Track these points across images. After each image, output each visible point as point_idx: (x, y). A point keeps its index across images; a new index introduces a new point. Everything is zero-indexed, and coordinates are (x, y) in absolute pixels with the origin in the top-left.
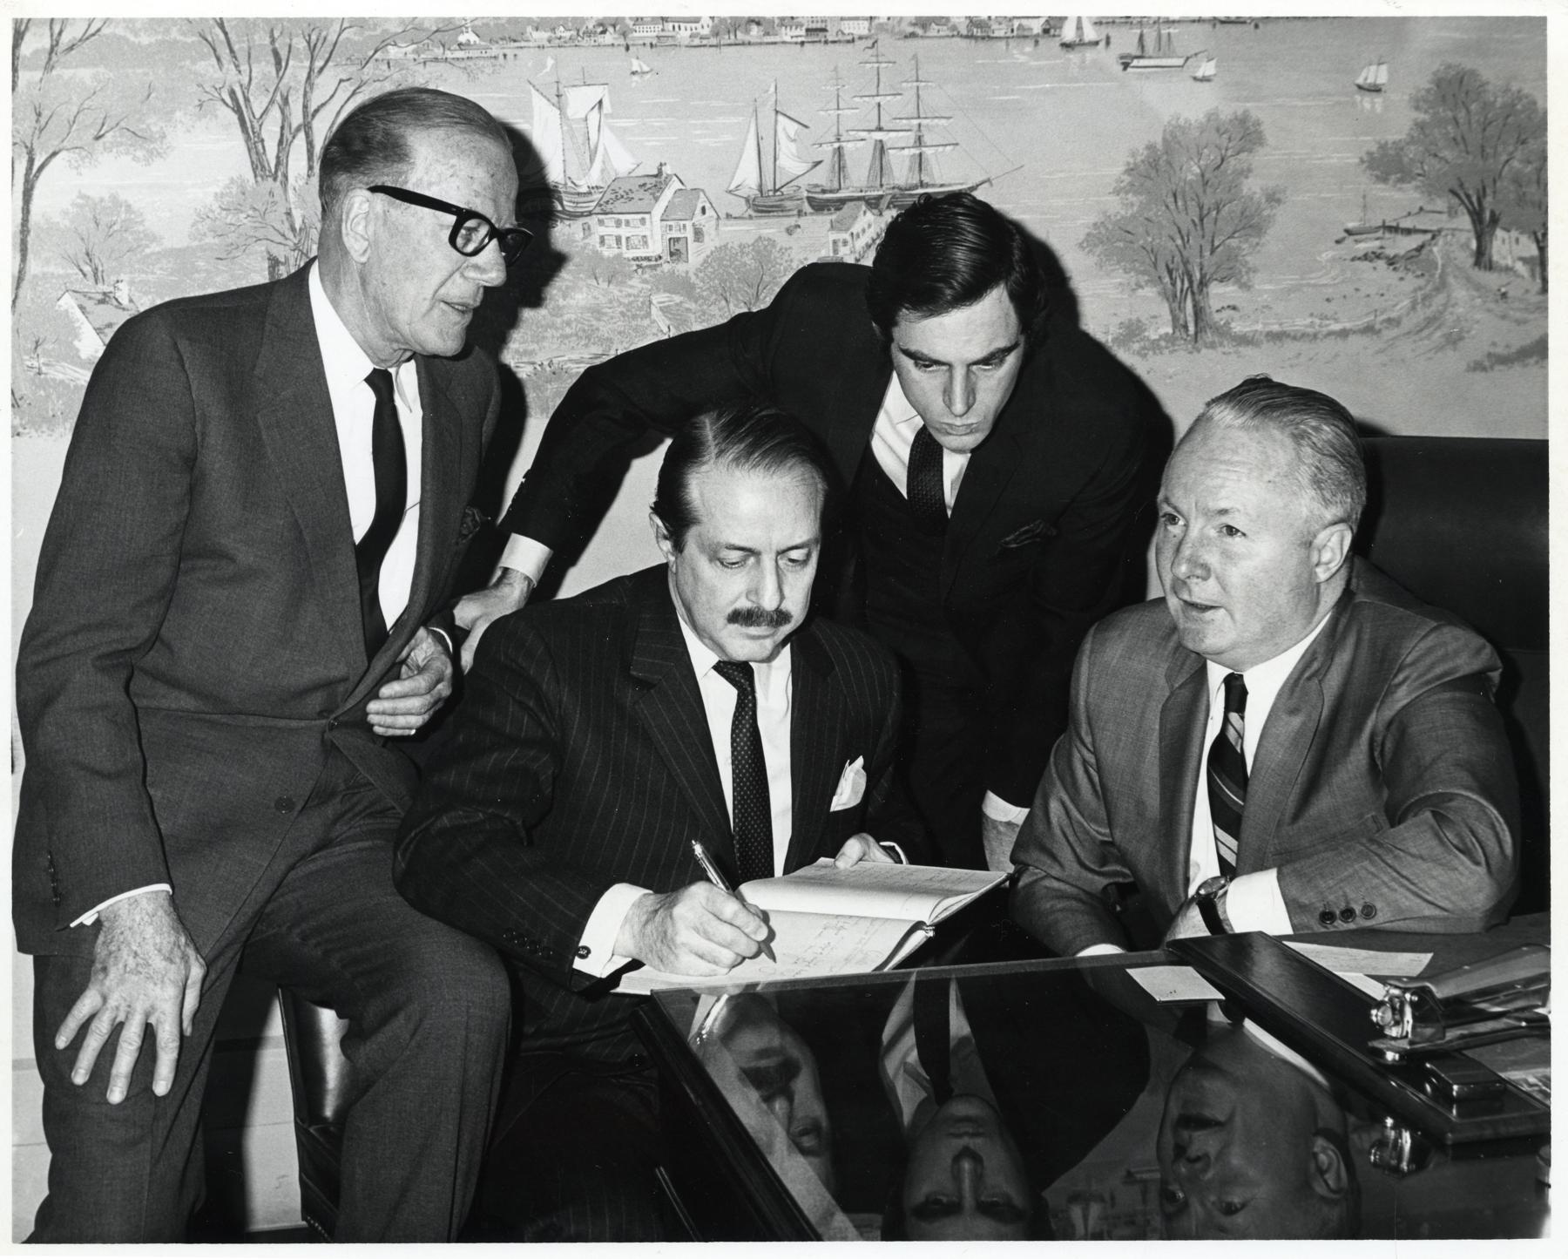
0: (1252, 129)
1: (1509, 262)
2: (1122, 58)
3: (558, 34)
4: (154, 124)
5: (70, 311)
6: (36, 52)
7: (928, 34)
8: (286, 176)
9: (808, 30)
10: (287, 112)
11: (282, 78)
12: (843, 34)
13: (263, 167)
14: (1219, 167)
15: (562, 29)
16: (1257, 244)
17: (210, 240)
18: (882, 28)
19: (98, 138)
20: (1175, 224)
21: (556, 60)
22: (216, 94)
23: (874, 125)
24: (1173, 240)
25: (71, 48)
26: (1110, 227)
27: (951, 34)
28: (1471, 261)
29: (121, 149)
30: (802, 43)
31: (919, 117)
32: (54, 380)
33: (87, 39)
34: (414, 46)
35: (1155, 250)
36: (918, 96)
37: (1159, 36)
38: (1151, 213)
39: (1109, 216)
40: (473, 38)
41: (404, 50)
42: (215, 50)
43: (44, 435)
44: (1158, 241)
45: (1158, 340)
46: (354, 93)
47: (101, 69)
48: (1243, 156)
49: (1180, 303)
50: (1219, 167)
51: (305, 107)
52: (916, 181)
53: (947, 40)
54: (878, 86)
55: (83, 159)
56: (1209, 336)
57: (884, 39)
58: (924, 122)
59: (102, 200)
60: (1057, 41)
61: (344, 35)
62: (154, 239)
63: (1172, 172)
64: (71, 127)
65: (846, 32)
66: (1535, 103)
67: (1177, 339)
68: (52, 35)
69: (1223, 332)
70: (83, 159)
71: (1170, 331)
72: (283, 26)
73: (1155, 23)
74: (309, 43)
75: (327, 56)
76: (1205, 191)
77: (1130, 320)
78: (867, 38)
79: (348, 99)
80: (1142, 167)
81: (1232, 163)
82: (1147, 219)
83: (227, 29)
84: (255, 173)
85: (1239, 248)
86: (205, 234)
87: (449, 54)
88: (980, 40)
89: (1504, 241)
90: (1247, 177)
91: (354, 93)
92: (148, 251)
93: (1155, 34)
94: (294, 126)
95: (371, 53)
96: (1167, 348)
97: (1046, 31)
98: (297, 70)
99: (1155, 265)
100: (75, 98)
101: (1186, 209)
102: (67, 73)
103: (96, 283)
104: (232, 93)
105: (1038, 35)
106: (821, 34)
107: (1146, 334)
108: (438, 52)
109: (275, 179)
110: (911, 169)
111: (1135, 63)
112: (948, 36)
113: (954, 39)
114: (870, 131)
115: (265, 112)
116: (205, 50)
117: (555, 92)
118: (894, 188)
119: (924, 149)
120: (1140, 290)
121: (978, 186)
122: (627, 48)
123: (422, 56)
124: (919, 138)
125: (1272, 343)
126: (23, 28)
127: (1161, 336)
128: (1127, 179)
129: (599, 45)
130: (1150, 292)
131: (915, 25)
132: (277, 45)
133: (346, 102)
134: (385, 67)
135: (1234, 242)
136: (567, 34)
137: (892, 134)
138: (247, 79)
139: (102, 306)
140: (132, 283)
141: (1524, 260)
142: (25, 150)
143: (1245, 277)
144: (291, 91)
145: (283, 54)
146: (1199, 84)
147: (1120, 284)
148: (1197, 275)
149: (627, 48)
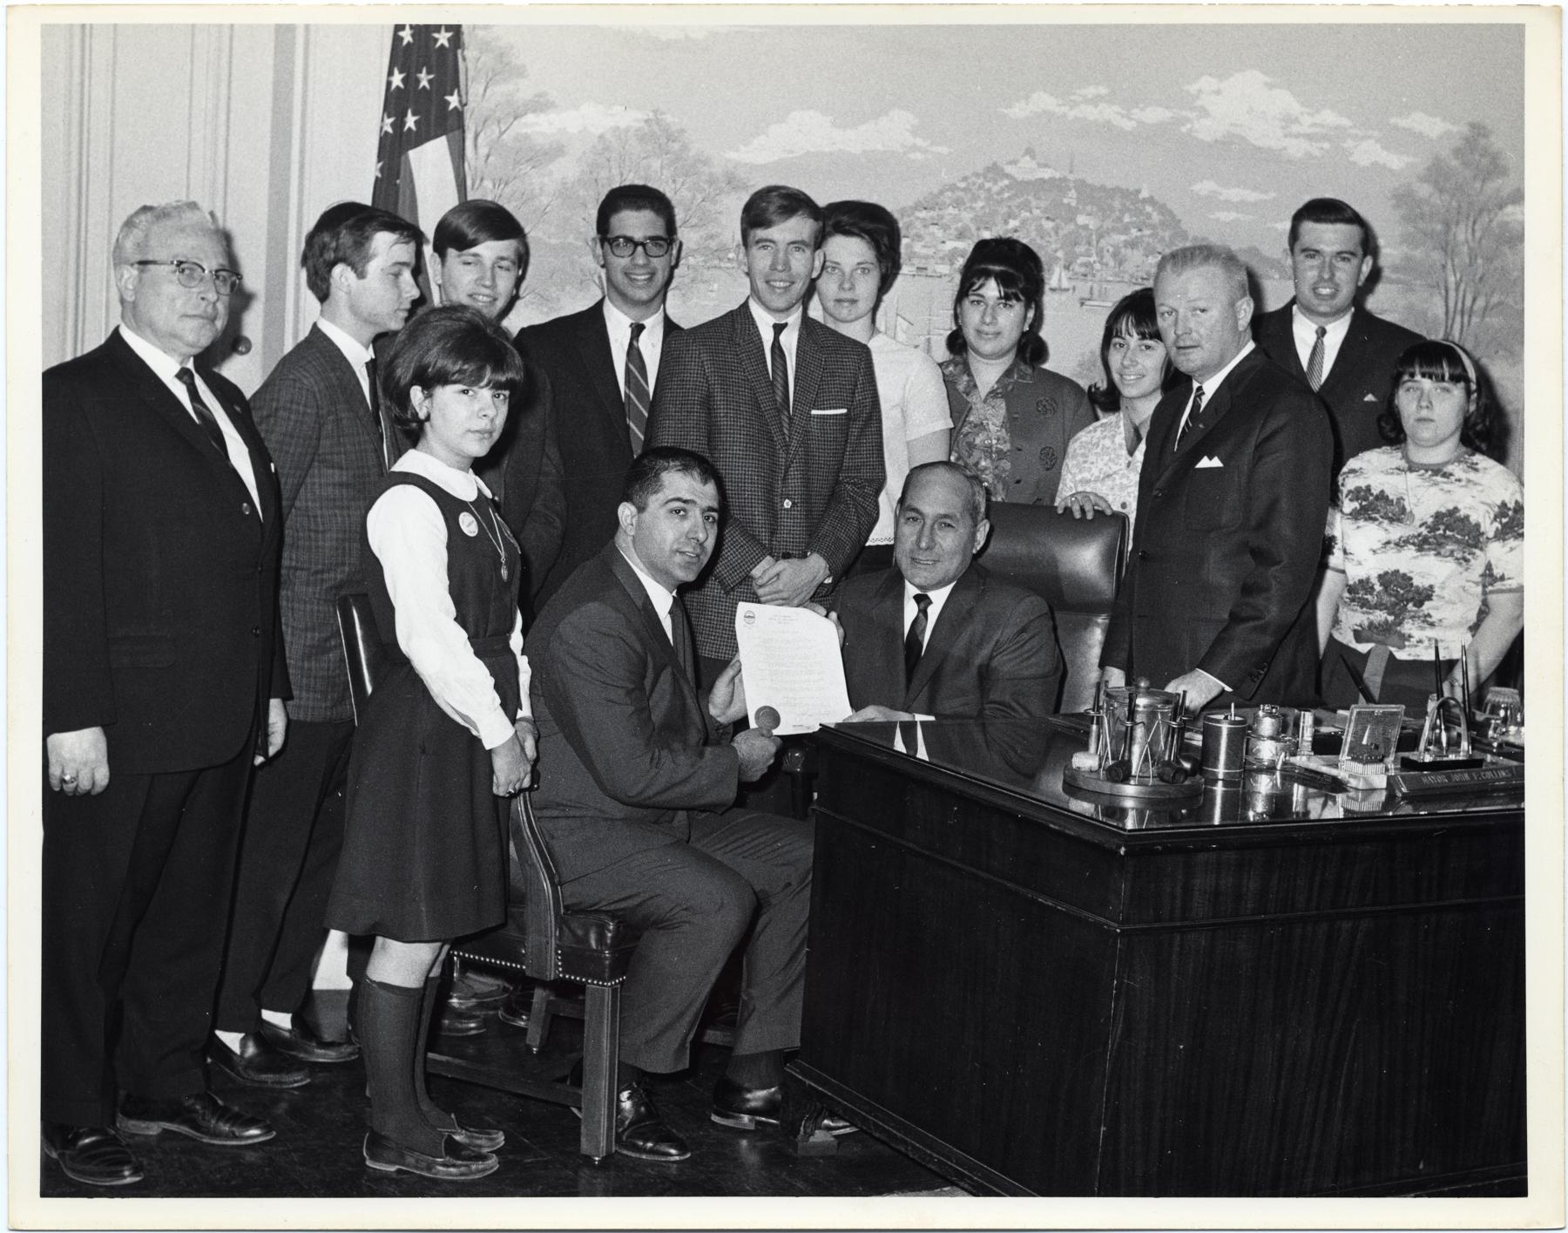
37: (1100, 291)
73: (1101, 281)
87: (722, 265)
106: (924, 273)
111: (1087, 303)
128: (1079, 369)
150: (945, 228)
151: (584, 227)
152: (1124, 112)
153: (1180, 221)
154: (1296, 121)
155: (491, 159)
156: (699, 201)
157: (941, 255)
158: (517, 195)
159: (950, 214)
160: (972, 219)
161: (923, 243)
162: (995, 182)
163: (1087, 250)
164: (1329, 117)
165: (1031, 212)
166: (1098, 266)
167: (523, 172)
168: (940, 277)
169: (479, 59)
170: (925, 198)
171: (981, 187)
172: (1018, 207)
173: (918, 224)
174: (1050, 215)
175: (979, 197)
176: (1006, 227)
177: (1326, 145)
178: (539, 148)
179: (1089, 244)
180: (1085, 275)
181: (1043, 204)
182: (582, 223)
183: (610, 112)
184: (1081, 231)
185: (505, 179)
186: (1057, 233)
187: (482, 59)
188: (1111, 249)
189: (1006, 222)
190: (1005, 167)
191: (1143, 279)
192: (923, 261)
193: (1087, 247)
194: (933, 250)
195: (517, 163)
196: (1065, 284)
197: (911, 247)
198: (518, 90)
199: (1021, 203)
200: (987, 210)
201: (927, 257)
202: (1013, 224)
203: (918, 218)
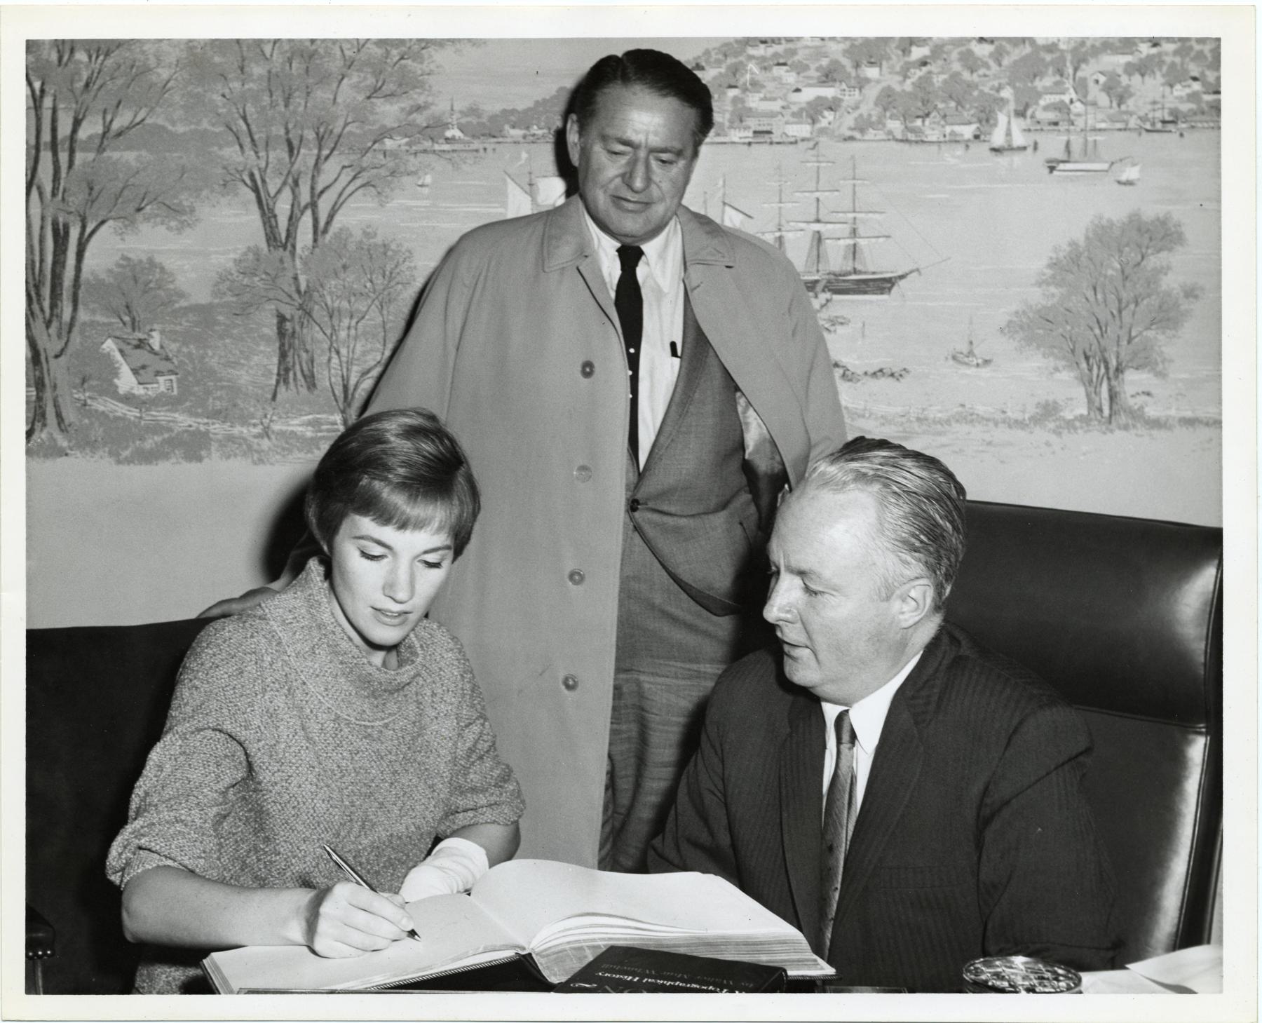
0: (1173, 229)
2: (1048, 162)
3: (532, 132)
4: (185, 199)
5: (112, 353)
6: (91, 137)
7: (866, 137)
8: (294, 247)
9: (755, 132)
10: (297, 190)
11: (292, 164)
12: (787, 136)
13: (275, 239)
14: (1139, 264)
15: (535, 127)
16: (1174, 336)
17: (229, 298)
18: (823, 131)
19: (139, 210)
20: (1094, 314)
21: (528, 152)
22: (238, 176)
23: (813, 218)
24: (1092, 329)
25: (119, 134)
26: (1031, 315)
27: (884, 137)
29: (159, 219)
30: (750, 144)
31: (854, 212)
32: (96, 411)
33: (134, 126)
34: (407, 140)
35: (1074, 339)
36: (854, 193)
38: (1071, 304)
39: (1031, 306)
40: (457, 133)
41: (399, 142)
42: (238, 138)
43: (88, 457)
44: (1077, 330)
45: (1073, 420)
46: (355, 178)
47: (144, 153)
48: (1164, 254)
49: (1096, 387)
50: (1139, 264)
51: (313, 188)
52: (849, 268)
53: (883, 143)
54: (818, 182)
55: (126, 226)
56: (1123, 419)
58: (858, 216)
59: (141, 261)
60: (986, 146)
61: (348, 129)
62: (181, 295)
63: (1092, 267)
64: (117, 199)
65: (790, 133)
67: (1091, 420)
68: (104, 123)
69: (1137, 416)
70: (126, 226)
71: (1085, 412)
72: (297, 121)
74: (317, 134)
75: (332, 145)
76: (1124, 286)
77: (1047, 401)
78: (808, 140)
79: (348, 185)
80: (1065, 262)
81: (1153, 261)
82: (1068, 310)
83: (250, 121)
84: (268, 240)
85: (1156, 338)
86: (225, 294)
87: (437, 147)
88: (914, 144)
90: (1166, 274)
91: (355, 178)
92: (177, 306)
93: (1081, 140)
94: (303, 204)
95: (369, 144)
96: (1082, 428)
97: (977, 137)
98: (307, 156)
99: (1073, 351)
100: (121, 176)
101: (1105, 301)
102: (116, 155)
103: (134, 330)
104: (252, 175)
105: (969, 140)
106: (767, 138)
107: (1062, 414)
109: (285, 247)
110: (845, 258)
111: (1062, 166)
113: (888, 143)
114: (808, 222)
115: (279, 192)
116: (230, 139)
117: (527, 180)
118: (829, 274)
119: (858, 240)
120: (1058, 374)
121: (907, 274)
123: (414, 148)
124: (854, 232)
125: (1184, 429)
126: (81, 117)
127: (1076, 418)
128: (1049, 272)
130: (1067, 376)
132: (291, 136)
133: (348, 185)
135: (1150, 334)
136: (540, 132)
137: (830, 226)
138: (263, 165)
139: (138, 351)
140: (162, 332)
142: (78, 218)
143: (1160, 367)
144: (302, 175)
145: (295, 143)
146: (1123, 187)
147: (1039, 368)
148: (1113, 363)
150: (800, 68)
151: (224, 106)
156: (397, 58)
157: (795, 109)
158: (123, 67)
160: (846, 52)
161: (762, 95)
163: (1057, 84)
166: (1078, 107)
168: (796, 142)
173: (752, 66)
176: (907, 59)
179: (1060, 72)
180: (1056, 124)
182: (217, 98)
184: (1043, 54)
186: (1000, 65)
188: (1102, 79)
191: (1164, 122)
192: (765, 121)
193: (1058, 78)
194: (780, 103)
196: (1019, 139)
197: (743, 101)
201: (772, 115)
203: (751, 57)
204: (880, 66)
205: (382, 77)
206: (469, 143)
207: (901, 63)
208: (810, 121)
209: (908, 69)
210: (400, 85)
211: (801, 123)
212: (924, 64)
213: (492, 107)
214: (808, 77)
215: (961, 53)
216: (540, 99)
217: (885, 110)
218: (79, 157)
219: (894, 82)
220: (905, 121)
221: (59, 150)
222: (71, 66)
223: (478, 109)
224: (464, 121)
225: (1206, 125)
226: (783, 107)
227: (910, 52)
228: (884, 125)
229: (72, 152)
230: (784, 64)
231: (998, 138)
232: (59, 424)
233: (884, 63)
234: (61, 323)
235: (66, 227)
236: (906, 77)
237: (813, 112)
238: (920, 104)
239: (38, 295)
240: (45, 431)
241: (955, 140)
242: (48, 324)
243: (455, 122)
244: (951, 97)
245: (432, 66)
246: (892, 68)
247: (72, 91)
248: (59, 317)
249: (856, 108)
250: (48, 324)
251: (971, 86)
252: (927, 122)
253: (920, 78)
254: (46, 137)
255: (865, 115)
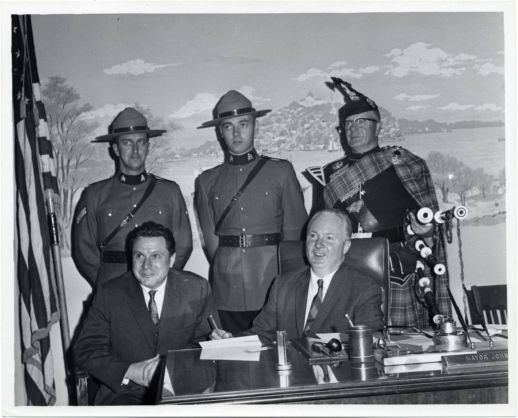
1: (452, 201)
6: (73, 165)
9: (263, 150)
15: (201, 153)
18: (282, 149)
25: (81, 163)
28: (442, 201)
34: (164, 159)
47: (89, 168)
57: (282, 151)
60: (327, 150)
65: (273, 150)
66: (456, 160)
87: (173, 160)
89: (450, 196)
95: (153, 161)
97: (324, 148)
102: (81, 169)
106: (266, 151)
108: (170, 160)
112: (298, 150)
117: (199, 168)
122: (217, 157)
129: (210, 156)
131: (290, 148)
134: (157, 164)
136: (202, 154)
141: (457, 200)
149: (217, 157)
150: (274, 132)
152: (355, 70)
153: (390, 113)
154: (446, 60)
155: (69, 132)
157: (273, 143)
158: (81, 144)
159: (275, 126)
160: (286, 127)
161: (264, 140)
162: (295, 110)
164: (463, 56)
165: (315, 120)
167: (83, 135)
168: (274, 153)
169: (60, 94)
170: (262, 121)
171: (289, 113)
172: (307, 119)
174: (324, 120)
175: (288, 117)
176: (303, 128)
177: (464, 69)
178: (88, 125)
181: (321, 115)
183: (116, 106)
185: (75, 140)
187: (62, 94)
189: (303, 125)
190: (299, 102)
195: (79, 132)
196: (336, 148)
197: (259, 142)
198: (77, 104)
199: (309, 116)
200: (293, 122)
201: (267, 145)
202: (306, 126)
204: (296, 131)
205: (156, 142)
206: (182, 158)
207: (302, 129)
208: (278, 146)
209: (304, 130)
210: (161, 143)
211: (275, 147)
212: (308, 129)
213: (188, 149)
214: (277, 134)
215: (318, 125)
216: (202, 145)
217: (298, 142)
218: (70, 170)
219: (300, 134)
220: (304, 144)
221: (64, 168)
222: (66, 145)
223: (184, 149)
224: (180, 152)
225: (386, 141)
226: (270, 143)
227: (304, 126)
228: (298, 146)
229: (68, 169)
230: (270, 131)
231: (330, 148)
232: (68, 248)
233: (297, 129)
234: (67, 218)
235: (67, 191)
236: (303, 133)
237: (279, 143)
238: (308, 140)
239: (60, 211)
240: (64, 250)
241: (318, 149)
242: (63, 219)
243: (178, 153)
244: (316, 137)
245: (170, 138)
246: (299, 130)
247: (67, 152)
248: (66, 217)
249: (290, 142)
250: (63, 219)
251: (322, 134)
252: (310, 145)
253: (307, 133)
254: (60, 165)
255: (293, 144)
